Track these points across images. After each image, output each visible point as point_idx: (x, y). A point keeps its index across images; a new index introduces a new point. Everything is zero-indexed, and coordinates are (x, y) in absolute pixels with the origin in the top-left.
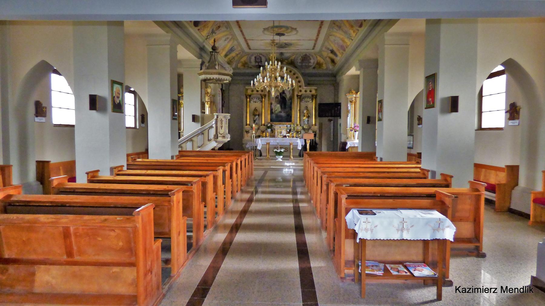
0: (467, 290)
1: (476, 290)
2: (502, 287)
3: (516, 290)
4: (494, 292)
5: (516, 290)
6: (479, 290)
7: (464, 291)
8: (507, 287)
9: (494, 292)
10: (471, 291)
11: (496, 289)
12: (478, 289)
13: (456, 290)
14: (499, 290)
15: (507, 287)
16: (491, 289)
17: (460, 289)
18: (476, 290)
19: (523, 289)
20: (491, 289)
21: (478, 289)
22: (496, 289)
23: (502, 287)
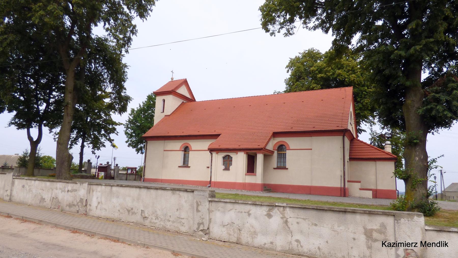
0: (392, 244)
1: (400, 244)
2: (421, 242)
3: (434, 244)
5: (434, 244)
6: (402, 244)
8: (426, 242)
11: (417, 243)
13: (383, 244)
14: (419, 245)
15: (426, 242)
16: (412, 243)
17: (386, 244)
18: (400, 244)
20: (412, 243)
21: (401, 244)
22: (417, 243)
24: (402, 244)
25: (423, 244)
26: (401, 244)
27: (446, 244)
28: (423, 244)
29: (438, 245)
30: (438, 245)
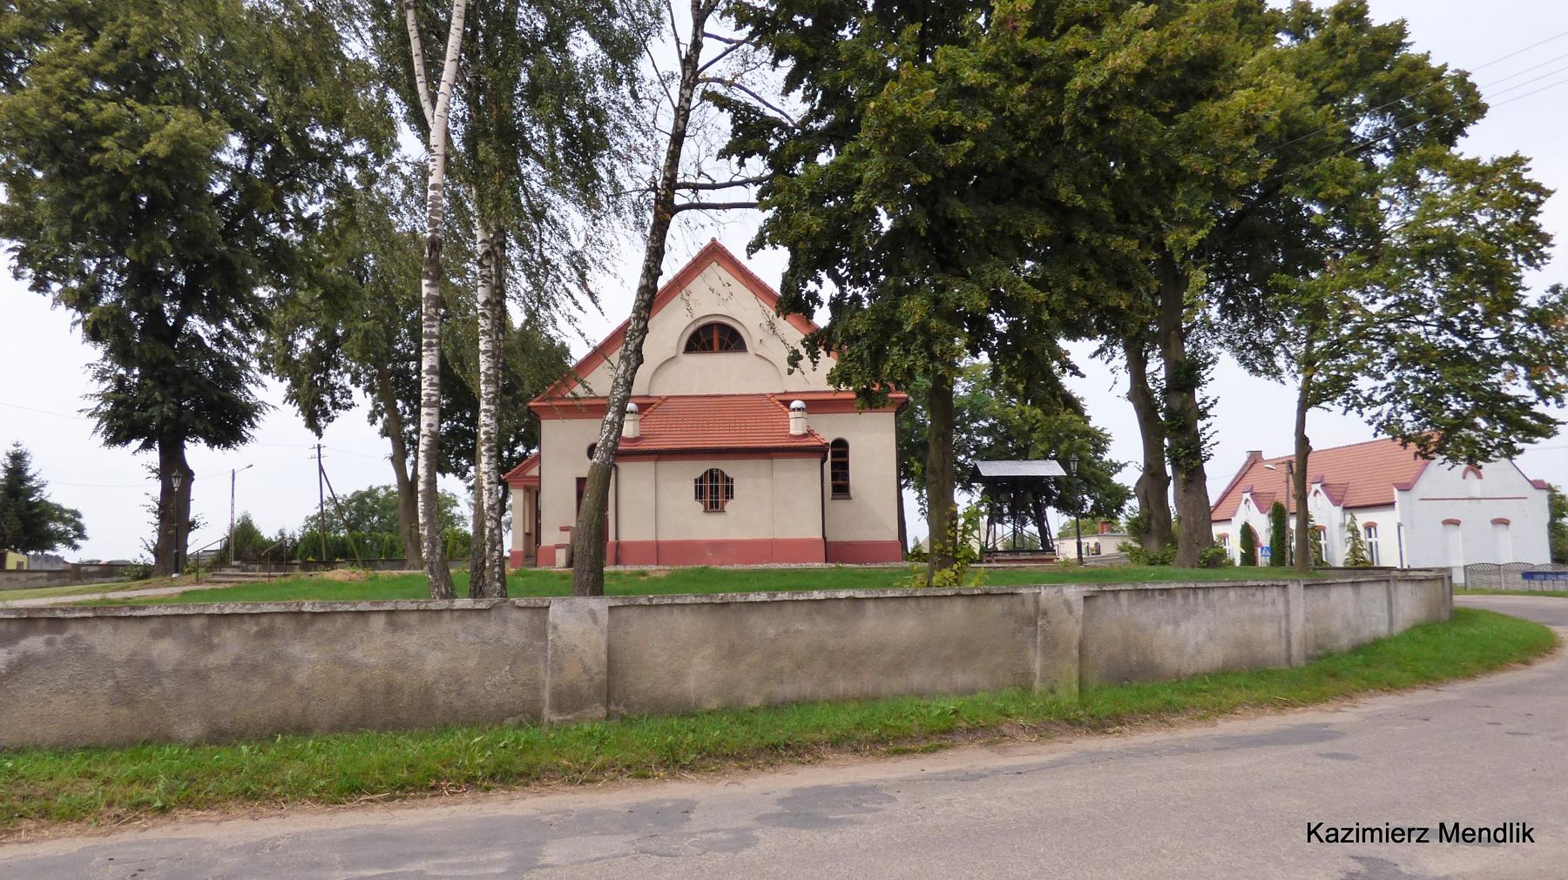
0: (1341, 834)
1: (1368, 833)
2: (1442, 826)
3: (1485, 833)
4: (1418, 841)
5: (1485, 833)
6: (1377, 833)
7: (1333, 836)
8: (1457, 825)
9: (1418, 841)
10: (1352, 836)
12: (1372, 831)
13: (1310, 833)
15: (1457, 825)
17: (1322, 832)
18: (1368, 833)
19: (1504, 830)
23: (1442, 826)
24: (1377, 833)
25: (1449, 828)
26: (1372, 831)
27: (1525, 834)
28: (1449, 828)
29: (1500, 835)
30: (1500, 835)
